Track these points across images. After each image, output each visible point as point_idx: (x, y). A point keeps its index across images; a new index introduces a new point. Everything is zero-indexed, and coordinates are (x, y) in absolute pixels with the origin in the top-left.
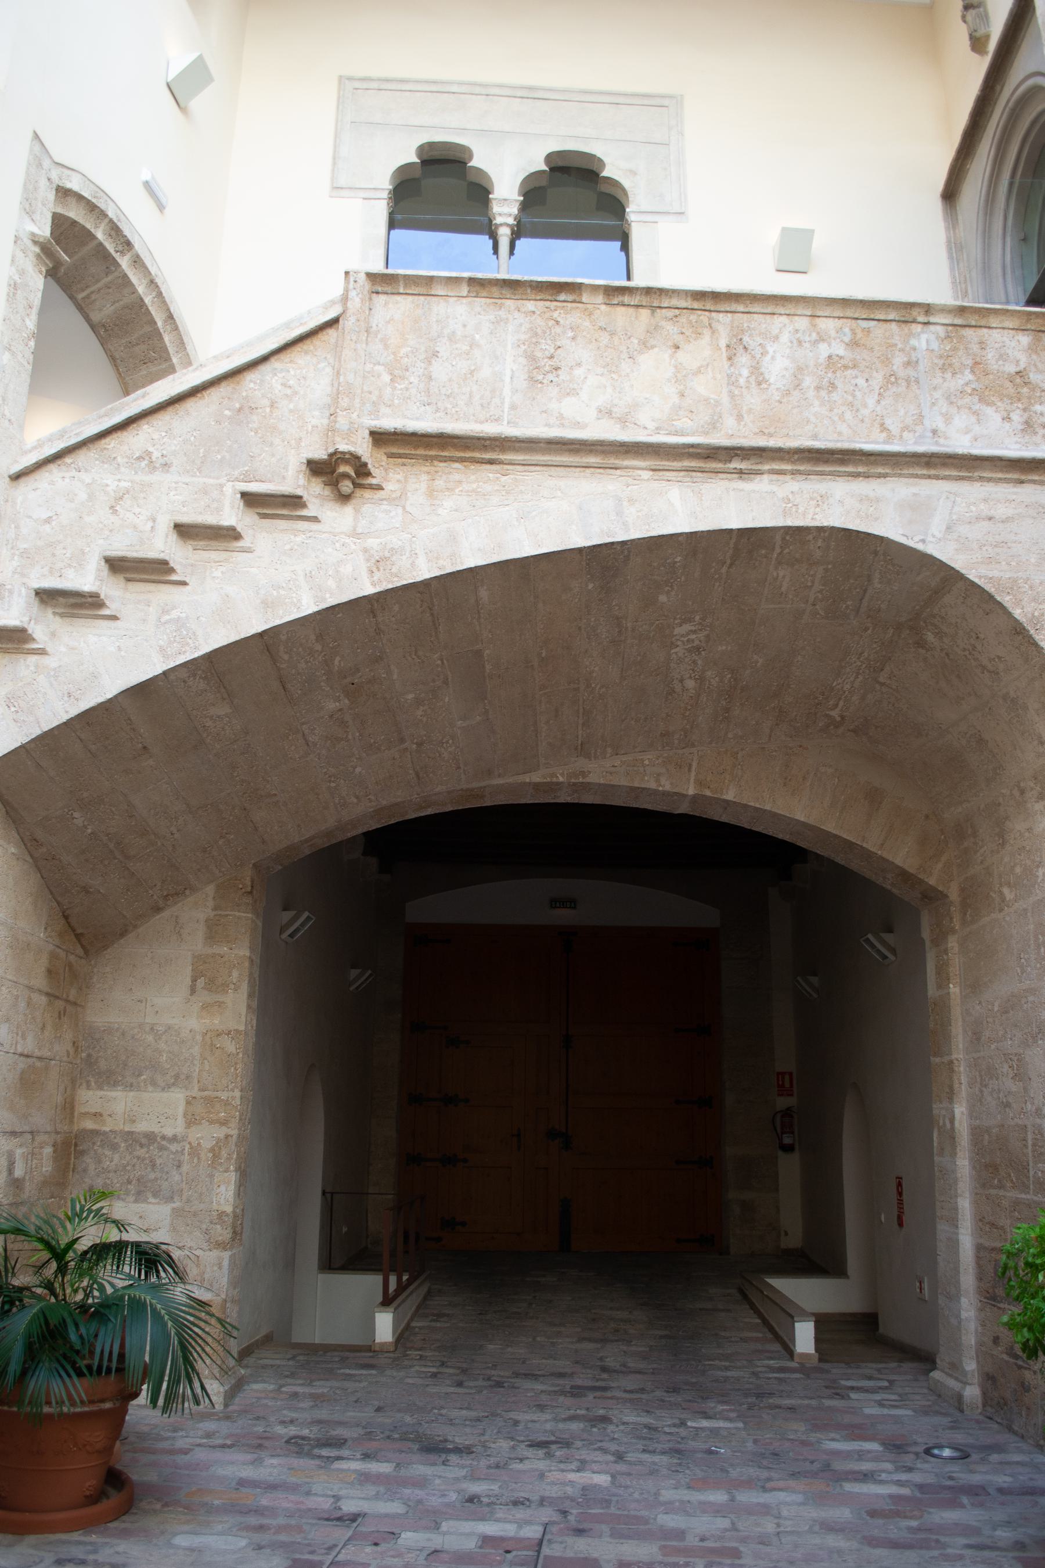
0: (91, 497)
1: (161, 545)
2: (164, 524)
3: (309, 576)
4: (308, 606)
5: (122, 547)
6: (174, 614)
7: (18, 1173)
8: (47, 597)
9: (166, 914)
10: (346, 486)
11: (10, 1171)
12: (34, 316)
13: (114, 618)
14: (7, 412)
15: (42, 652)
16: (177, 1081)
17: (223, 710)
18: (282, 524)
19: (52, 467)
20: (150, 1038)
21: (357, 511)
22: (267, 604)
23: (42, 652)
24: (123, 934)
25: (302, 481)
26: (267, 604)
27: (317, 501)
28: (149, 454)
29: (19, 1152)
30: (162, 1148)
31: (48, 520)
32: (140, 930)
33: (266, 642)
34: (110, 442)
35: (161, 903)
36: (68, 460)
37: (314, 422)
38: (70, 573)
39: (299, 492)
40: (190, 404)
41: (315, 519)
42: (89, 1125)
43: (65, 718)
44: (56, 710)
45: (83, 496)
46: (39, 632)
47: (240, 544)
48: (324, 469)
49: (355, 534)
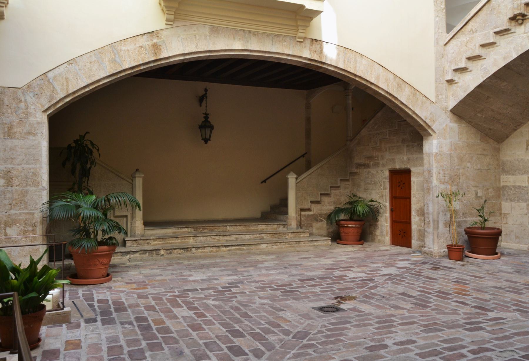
0: (461, 44)
1: (478, 51)
2: (478, 45)
3: (514, 48)
4: (514, 56)
5: (469, 55)
6: (484, 66)
7: (479, 195)
8: (456, 70)
9: (518, 130)
10: (520, 21)
11: (476, 194)
12: (444, 4)
13: (471, 71)
14: (440, 31)
15: (457, 83)
16: (525, 173)
17: (505, 83)
18: (506, 36)
19: (452, 40)
20: (517, 162)
21: (525, 26)
22: (505, 58)
23: (457, 83)
24: (507, 137)
25: (508, 24)
26: (505, 58)
27: (514, 27)
28: (472, 29)
29: (479, 191)
30: (523, 189)
31: (453, 53)
32: (512, 135)
33: (507, 67)
34: (464, 29)
35: (515, 128)
36: (455, 37)
37: (510, 6)
38: (459, 64)
39: (508, 28)
40: (480, 13)
41: (514, 32)
42: (504, 184)
43: (464, 96)
44: (462, 95)
45: (460, 44)
46: (456, 79)
47: (496, 45)
48: (514, 19)
49: (525, 33)
